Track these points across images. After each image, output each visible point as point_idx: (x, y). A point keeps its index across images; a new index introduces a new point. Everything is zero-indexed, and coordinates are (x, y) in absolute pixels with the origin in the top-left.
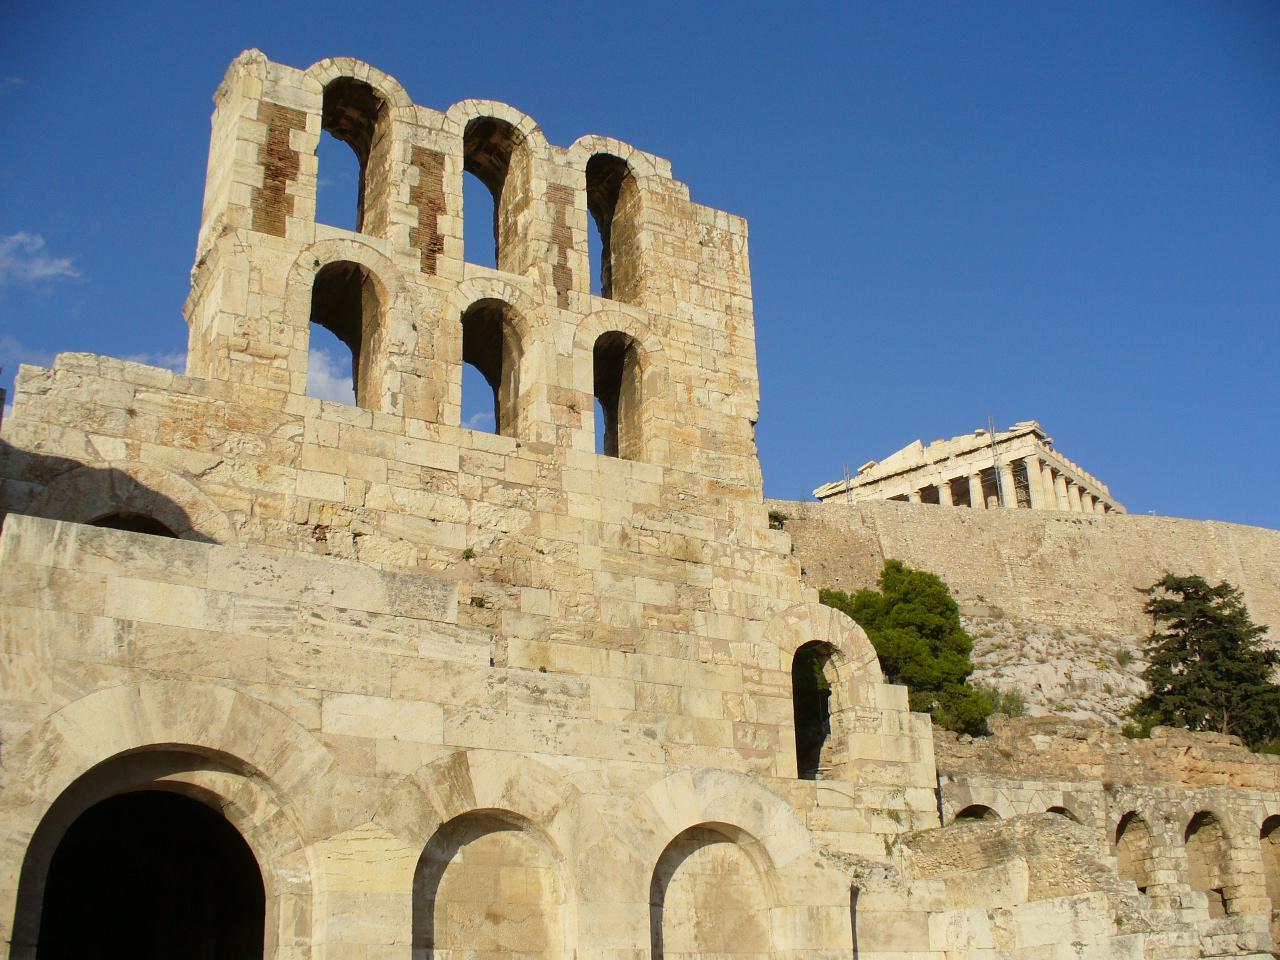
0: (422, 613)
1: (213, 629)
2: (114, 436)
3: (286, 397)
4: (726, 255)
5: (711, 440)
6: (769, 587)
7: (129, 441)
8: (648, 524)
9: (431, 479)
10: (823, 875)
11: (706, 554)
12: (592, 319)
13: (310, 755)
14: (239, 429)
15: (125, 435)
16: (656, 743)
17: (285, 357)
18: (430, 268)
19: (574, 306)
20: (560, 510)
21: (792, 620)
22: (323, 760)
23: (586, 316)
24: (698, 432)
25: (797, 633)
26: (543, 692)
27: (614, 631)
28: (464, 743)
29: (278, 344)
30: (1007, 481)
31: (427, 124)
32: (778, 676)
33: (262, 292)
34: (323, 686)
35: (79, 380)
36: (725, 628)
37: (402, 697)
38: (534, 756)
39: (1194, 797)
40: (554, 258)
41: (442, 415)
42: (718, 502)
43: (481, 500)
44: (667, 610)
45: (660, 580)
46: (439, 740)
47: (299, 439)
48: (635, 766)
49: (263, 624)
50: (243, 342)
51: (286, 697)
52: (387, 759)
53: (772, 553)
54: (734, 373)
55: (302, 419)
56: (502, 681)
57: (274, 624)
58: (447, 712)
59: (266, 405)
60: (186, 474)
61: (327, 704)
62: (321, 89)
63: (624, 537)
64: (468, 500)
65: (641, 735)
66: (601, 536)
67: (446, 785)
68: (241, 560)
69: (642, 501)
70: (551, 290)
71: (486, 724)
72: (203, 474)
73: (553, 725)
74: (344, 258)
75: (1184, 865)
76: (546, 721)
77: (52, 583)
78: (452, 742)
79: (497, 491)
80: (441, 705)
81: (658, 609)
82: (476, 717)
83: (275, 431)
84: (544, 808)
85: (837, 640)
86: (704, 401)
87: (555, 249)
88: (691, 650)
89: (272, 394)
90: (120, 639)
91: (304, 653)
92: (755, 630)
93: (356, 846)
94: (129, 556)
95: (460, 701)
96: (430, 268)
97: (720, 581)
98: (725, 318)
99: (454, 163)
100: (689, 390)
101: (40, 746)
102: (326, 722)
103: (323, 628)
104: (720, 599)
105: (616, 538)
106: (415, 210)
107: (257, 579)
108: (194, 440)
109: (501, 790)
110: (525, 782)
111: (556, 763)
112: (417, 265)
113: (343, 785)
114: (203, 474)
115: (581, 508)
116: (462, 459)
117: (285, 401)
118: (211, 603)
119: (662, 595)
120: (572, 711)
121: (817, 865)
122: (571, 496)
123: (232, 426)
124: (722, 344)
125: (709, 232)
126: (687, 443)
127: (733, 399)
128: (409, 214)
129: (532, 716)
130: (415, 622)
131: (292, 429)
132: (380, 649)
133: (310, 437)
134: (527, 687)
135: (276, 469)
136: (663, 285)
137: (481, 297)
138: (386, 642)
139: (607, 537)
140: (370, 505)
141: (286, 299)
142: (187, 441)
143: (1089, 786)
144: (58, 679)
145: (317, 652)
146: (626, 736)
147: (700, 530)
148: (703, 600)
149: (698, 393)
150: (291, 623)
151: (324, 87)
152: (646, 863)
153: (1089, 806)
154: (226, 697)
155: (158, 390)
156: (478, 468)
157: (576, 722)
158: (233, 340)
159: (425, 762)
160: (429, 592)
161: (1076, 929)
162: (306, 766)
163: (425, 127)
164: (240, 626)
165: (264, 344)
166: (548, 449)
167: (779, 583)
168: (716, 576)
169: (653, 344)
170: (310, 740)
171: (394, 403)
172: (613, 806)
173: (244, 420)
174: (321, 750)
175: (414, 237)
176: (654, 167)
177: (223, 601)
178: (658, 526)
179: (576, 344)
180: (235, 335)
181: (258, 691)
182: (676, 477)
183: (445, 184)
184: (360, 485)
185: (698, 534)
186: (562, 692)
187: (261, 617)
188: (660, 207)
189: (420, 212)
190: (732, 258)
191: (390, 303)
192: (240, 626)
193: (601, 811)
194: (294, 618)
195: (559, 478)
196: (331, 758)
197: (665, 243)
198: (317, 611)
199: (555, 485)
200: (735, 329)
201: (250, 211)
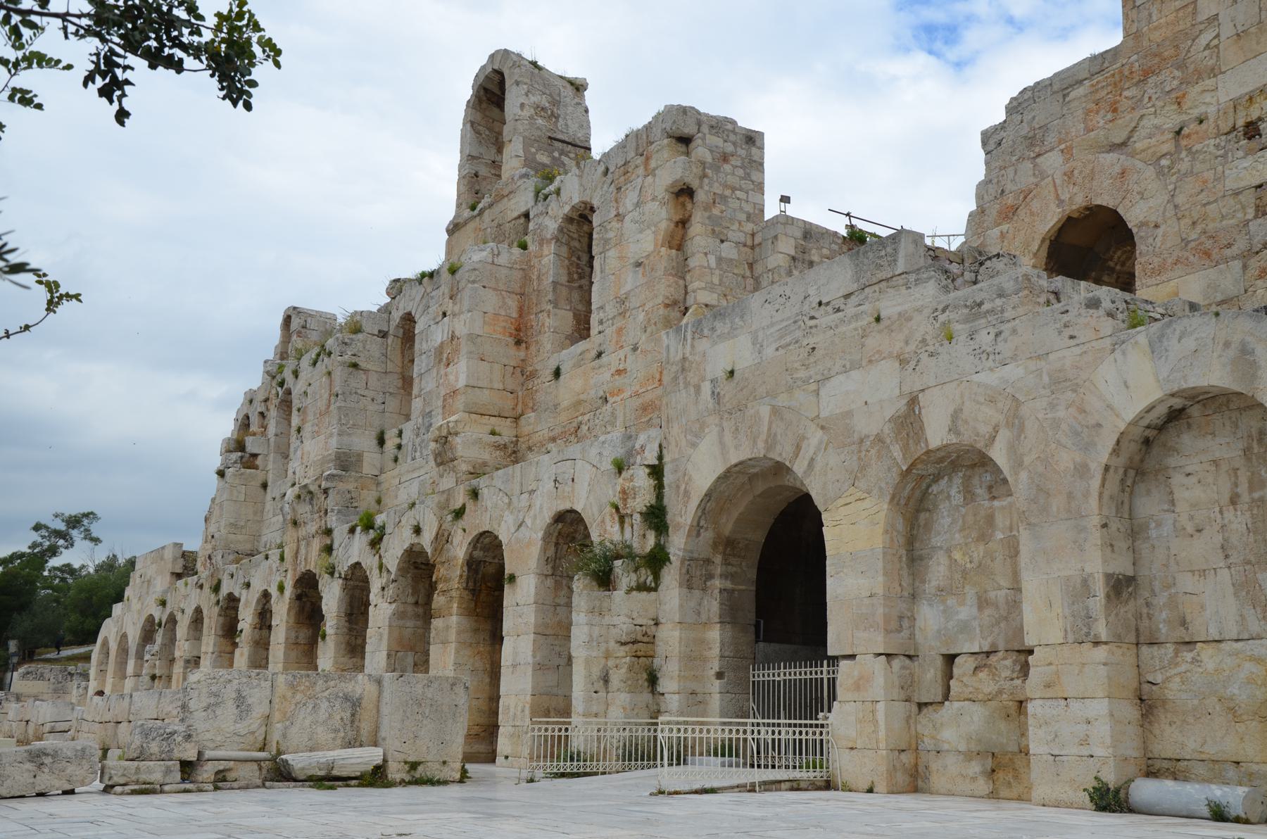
7: (1063, 146)
13: (815, 437)
15: (1060, 143)
16: (1101, 312)
34: (819, 377)
35: (1019, 118)
37: (870, 361)
38: (976, 378)
46: (897, 392)
47: (1216, 42)
48: (1077, 350)
49: (783, 342)
56: (944, 311)
59: (1177, 29)
61: (822, 393)
65: (1083, 311)
72: (1129, 138)
73: (992, 336)
76: (985, 339)
77: (683, 370)
78: (906, 389)
82: (924, 357)
83: (1189, 51)
84: (985, 430)
89: (1181, 14)
93: (843, 511)
101: (683, 487)
107: (777, 306)
108: (1115, 110)
114: (1129, 138)
117: (1195, 13)
120: (1009, 314)
123: (1147, 73)
130: (876, 288)
131: (1204, 40)
132: (853, 325)
134: (966, 306)
135: (1194, 91)
138: (856, 317)
142: (1109, 116)
144: (689, 437)
145: (814, 349)
146: (1066, 318)
150: (798, 334)
152: (1093, 466)
154: (765, 411)
155: (1081, 82)
157: (1013, 323)
160: (883, 253)
172: (1053, 406)
173: (1157, 60)
174: (820, 433)
177: (761, 334)
181: (782, 400)
186: (1000, 296)
187: (781, 337)
192: (769, 351)
193: (1040, 416)
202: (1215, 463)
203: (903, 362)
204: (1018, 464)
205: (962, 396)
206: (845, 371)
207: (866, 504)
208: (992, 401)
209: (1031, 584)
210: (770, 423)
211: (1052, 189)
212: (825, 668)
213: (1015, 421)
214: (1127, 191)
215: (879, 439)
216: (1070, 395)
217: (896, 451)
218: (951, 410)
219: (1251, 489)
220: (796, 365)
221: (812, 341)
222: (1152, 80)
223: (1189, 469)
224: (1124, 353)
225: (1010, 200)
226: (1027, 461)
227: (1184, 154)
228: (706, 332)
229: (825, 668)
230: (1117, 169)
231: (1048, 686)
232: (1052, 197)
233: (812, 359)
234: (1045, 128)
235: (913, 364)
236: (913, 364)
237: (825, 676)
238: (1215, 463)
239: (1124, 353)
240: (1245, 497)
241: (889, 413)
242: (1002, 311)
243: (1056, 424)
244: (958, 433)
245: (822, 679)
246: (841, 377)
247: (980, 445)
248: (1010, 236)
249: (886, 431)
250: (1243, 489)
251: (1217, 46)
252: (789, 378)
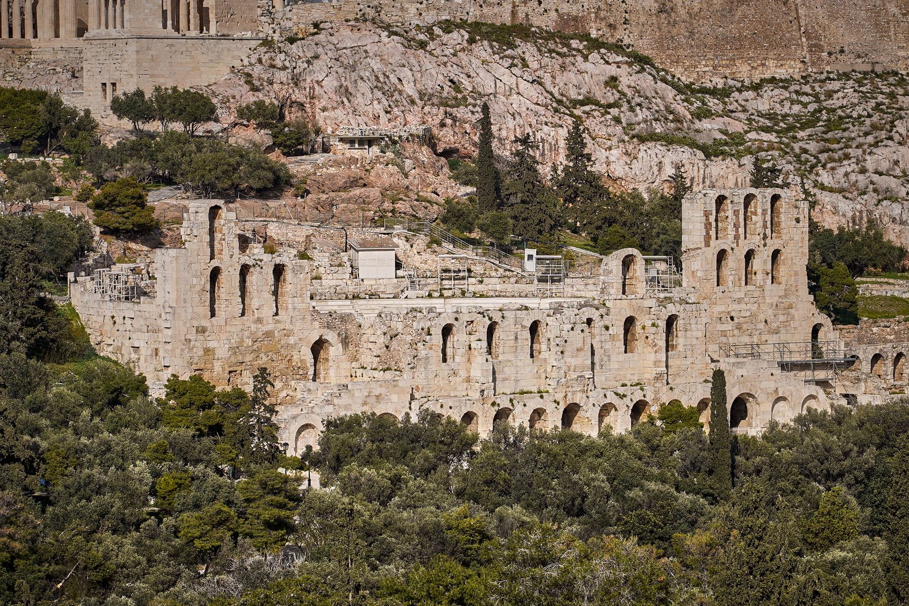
36: (797, 324)
45: (784, 314)
92: (804, 323)
104: (796, 317)
115: (768, 301)
147: (793, 299)
148: (793, 318)
165: (709, 277)
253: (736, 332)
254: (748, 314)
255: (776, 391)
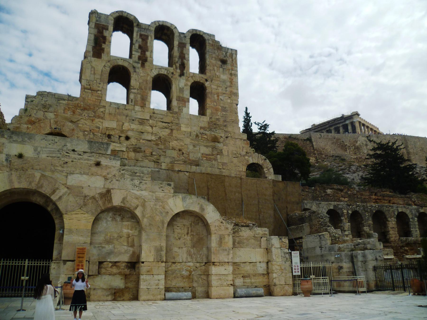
0: (100, 152)
1: (35, 157)
2: (51, 112)
3: (101, 101)
4: (231, 60)
5: (224, 109)
6: (240, 148)
8: (204, 132)
9: (142, 122)
10: (223, 226)
11: (221, 140)
12: (190, 78)
14: (87, 110)
15: (54, 112)
16: (171, 187)
17: (101, 91)
18: (143, 65)
19: (185, 75)
20: (179, 129)
21: (246, 157)
22: (66, 192)
23: (188, 77)
24: (220, 108)
25: (248, 161)
26: (136, 173)
27: (193, 161)
28: (111, 187)
29: (99, 87)
30: (350, 127)
31: (144, 27)
32: (242, 172)
33: (94, 74)
34: (68, 172)
35: (42, 98)
36: (225, 160)
37: (92, 174)
38: (132, 191)
39: (375, 207)
40: (180, 62)
41: (145, 105)
42: (225, 126)
43: (156, 127)
44: (209, 155)
45: (207, 147)
46: (103, 186)
47: (104, 112)
48: (164, 194)
49: (51, 155)
50: (89, 87)
51: (57, 175)
52: (86, 192)
53: (241, 139)
54: (231, 92)
55: (105, 106)
56: (123, 170)
57: (54, 155)
58: (105, 179)
60: (72, 122)
61: (69, 177)
62: (113, 19)
63: (197, 136)
64: (152, 127)
66: (190, 135)
67: (104, 199)
68: (45, 138)
69: (203, 125)
70: (179, 71)
71: (117, 182)
73: (139, 182)
74: (118, 64)
75: (372, 226)
76: (137, 182)
78: (106, 186)
79: (160, 124)
80: (104, 177)
81: (207, 155)
82: (114, 181)
84: (134, 205)
85: (261, 162)
86: (222, 99)
87: (180, 60)
88: (216, 166)
90: (7, 160)
91: (63, 163)
92: (235, 160)
93: (74, 216)
94: (11, 137)
95: (110, 176)
96: (143, 65)
97: (225, 147)
98: (229, 76)
99: (151, 38)
100: (218, 96)
102: (68, 181)
103: (69, 156)
104: (225, 153)
105: (195, 136)
106: (140, 51)
107: (50, 143)
108: (74, 113)
109: (121, 200)
110: (129, 198)
111: (138, 193)
112: (139, 65)
113: (71, 199)
114: (76, 121)
116: (151, 117)
117: (100, 102)
118: (35, 150)
119: (207, 151)
120: (145, 179)
121: (222, 223)
122: (182, 125)
123: (84, 109)
124: (228, 84)
125: (226, 54)
126: (217, 110)
127: (231, 98)
128: (138, 52)
129: (132, 180)
130: (98, 155)
131: (102, 110)
132: (86, 162)
133: (107, 111)
135: (97, 120)
136: (211, 68)
137: (157, 73)
138: (88, 160)
139: (192, 136)
140: (123, 129)
141: (101, 75)
142: (72, 113)
143: (342, 203)
146: (161, 185)
147: (220, 134)
148: (220, 153)
149: (220, 97)
150: (59, 155)
151: (114, 18)
152: (165, 221)
153: (342, 209)
154: (38, 175)
155: (64, 100)
156: (155, 118)
158: (86, 86)
159: (98, 192)
160: (102, 146)
161: (320, 243)
162: (61, 194)
163: (143, 28)
164: (43, 156)
165: (95, 87)
166: (176, 113)
167: (243, 147)
168: (224, 145)
169: (208, 84)
170: (63, 187)
171: (132, 102)
172: (155, 205)
175: (139, 58)
176: (210, 36)
177: (39, 149)
178: (207, 132)
179: (186, 85)
180: (87, 85)
181: (47, 174)
182: (213, 120)
183: (148, 43)
184: (121, 123)
185: (219, 135)
186: (143, 173)
187: (50, 153)
188: (211, 47)
189: (141, 51)
190: (232, 60)
191: (132, 75)
193: (152, 206)
194: (60, 154)
195: (179, 120)
196: (69, 192)
197: (212, 57)
198: (68, 151)
199: (177, 122)
200: (232, 79)
201: (92, 52)
202: (184, 225)
203: (106, 179)
204: (144, 216)
205: (127, 194)
206: (81, 174)
207: (86, 215)
208: (137, 198)
209: (145, 247)
210: (40, 178)
211: (49, 123)
212: (27, 262)
213: (144, 206)
214: (73, 135)
215: (93, 198)
216: (161, 203)
217: (100, 202)
218: (122, 197)
219: (191, 232)
220: (58, 165)
221: (66, 160)
222: (86, 111)
223: (178, 225)
224: (176, 198)
225: (33, 119)
226: (147, 216)
227: (91, 133)
228: (6, 136)
229: (27, 262)
230: (72, 128)
231: (148, 272)
232: (49, 125)
233: (65, 165)
234: (50, 106)
235: (110, 181)
236: (110, 181)
237: (26, 264)
238: (184, 225)
239: (176, 198)
240: (190, 234)
241: (99, 191)
242: (143, 177)
243: (156, 209)
244: (124, 204)
245: (24, 266)
246: (79, 175)
247: (132, 208)
248: (31, 129)
249: (97, 196)
250: (190, 231)
251: (104, 113)
252: (53, 168)
253: (132, 155)
254: (153, 138)
255: (107, 194)
